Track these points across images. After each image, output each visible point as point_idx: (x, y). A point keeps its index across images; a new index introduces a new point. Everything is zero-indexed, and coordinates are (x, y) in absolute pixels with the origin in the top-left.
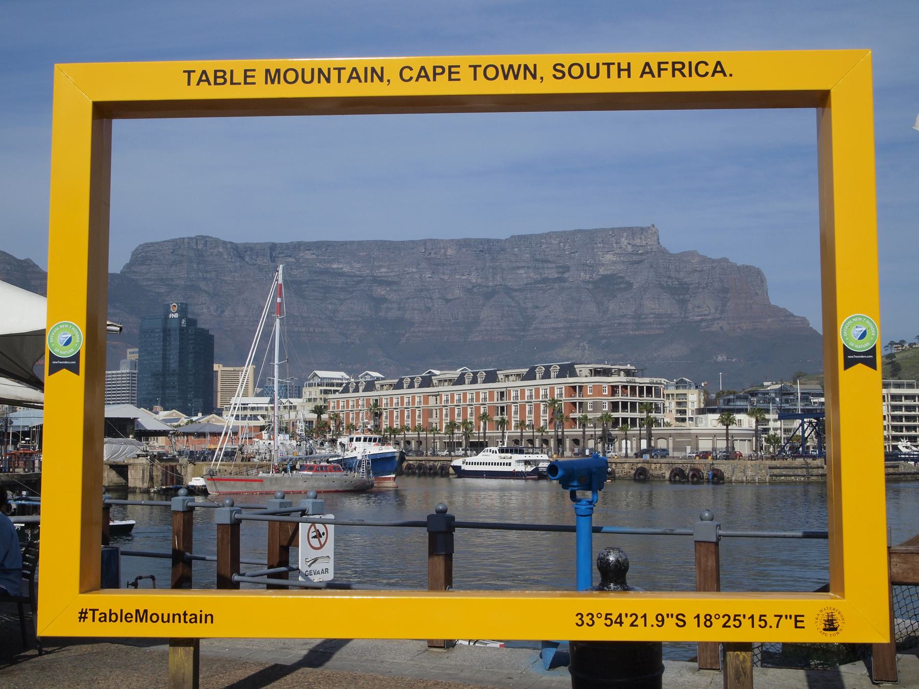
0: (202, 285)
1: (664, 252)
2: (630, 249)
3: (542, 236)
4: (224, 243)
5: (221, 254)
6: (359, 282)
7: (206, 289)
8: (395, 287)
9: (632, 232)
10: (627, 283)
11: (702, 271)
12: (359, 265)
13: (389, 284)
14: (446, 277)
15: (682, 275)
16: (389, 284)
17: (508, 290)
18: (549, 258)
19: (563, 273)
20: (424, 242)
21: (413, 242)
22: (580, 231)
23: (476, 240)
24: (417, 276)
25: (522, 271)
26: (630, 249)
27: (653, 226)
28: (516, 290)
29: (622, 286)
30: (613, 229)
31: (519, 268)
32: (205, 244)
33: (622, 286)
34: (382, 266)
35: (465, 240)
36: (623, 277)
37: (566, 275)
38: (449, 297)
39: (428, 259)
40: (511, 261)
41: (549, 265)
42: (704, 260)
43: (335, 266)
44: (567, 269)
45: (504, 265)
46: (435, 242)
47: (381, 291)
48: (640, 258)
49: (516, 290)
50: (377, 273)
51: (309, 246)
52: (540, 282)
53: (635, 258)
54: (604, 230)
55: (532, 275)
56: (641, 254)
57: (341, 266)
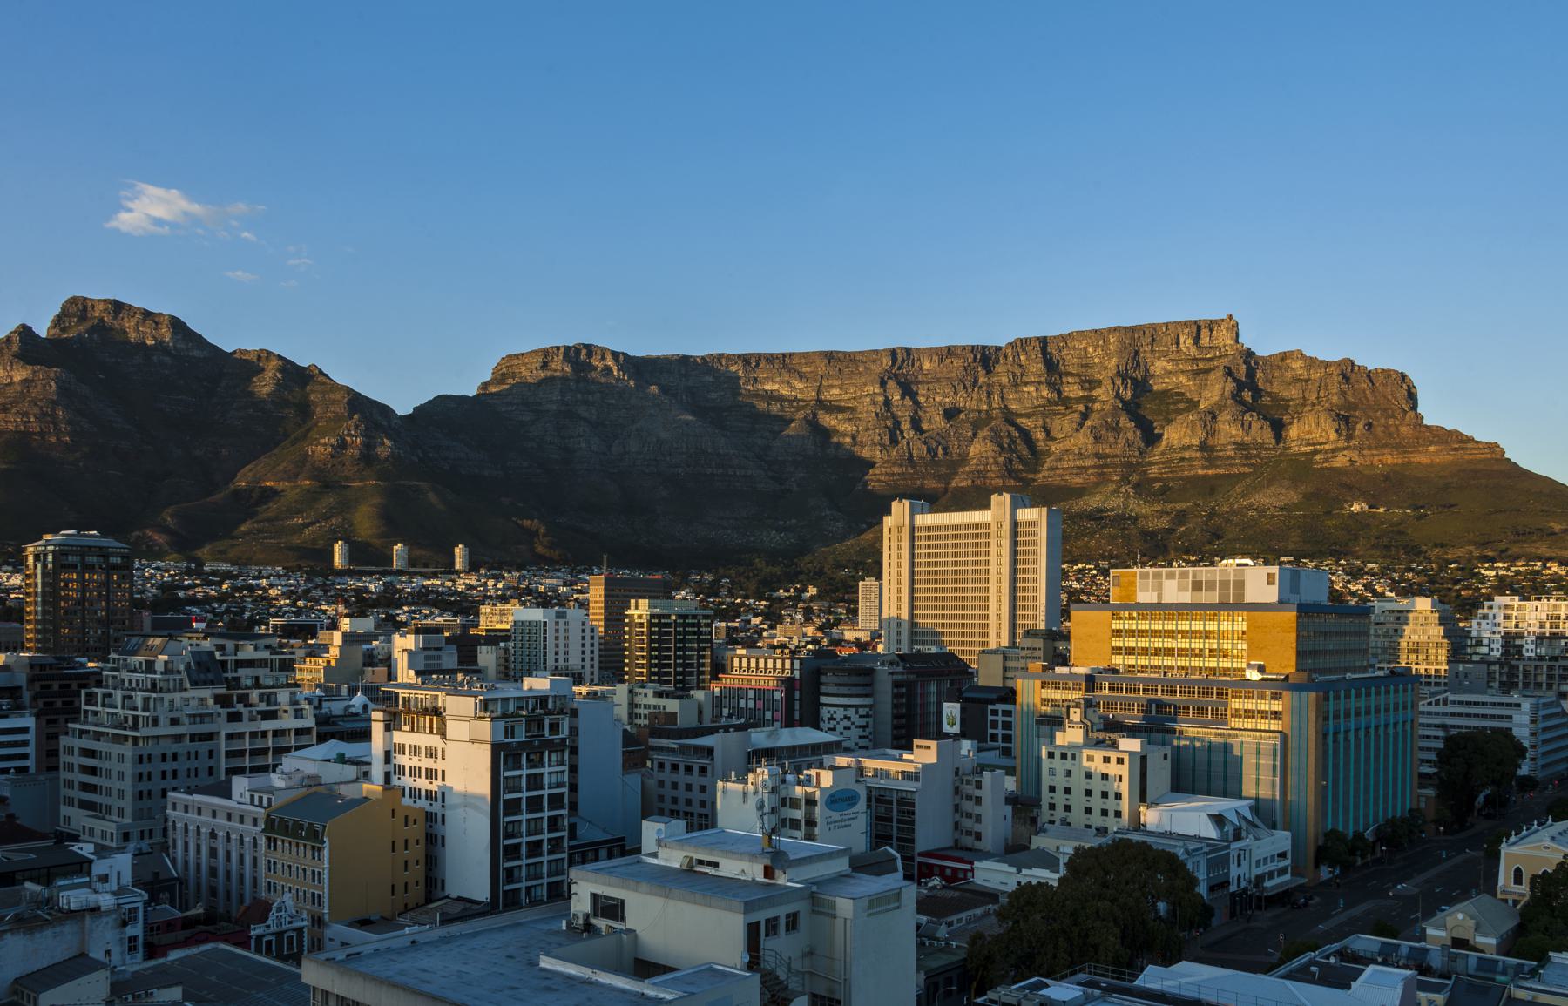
0: (582, 411)
1: (1249, 354)
2: (1194, 351)
3: (1063, 338)
4: (615, 355)
5: (608, 370)
6: (803, 408)
7: (585, 414)
8: (847, 415)
9: (1197, 328)
10: (1190, 401)
11: (1307, 381)
12: (800, 386)
13: (841, 410)
14: (922, 400)
15: (1275, 389)
16: (841, 410)
17: (1009, 417)
18: (1070, 369)
19: (1091, 389)
20: (893, 353)
21: (876, 352)
22: (1115, 329)
23: (964, 348)
24: (881, 399)
25: (1032, 389)
26: (1194, 351)
27: (1231, 317)
28: (1021, 416)
29: (1182, 406)
30: (1167, 325)
31: (1026, 384)
32: (590, 355)
33: (1182, 406)
34: (832, 387)
35: (949, 348)
36: (1182, 394)
37: (1094, 393)
38: (925, 426)
39: (896, 376)
40: (1014, 375)
41: (1070, 380)
42: (1311, 363)
43: (768, 387)
44: (1099, 383)
45: (1005, 380)
46: (908, 351)
47: (828, 420)
48: (1211, 365)
49: (1021, 416)
50: (826, 396)
51: (731, 358)
52: (1056, 404)
53: (1201, 366)
54: (1154, 327)
55: (1045, 392)
56: (1211, 359)
57: (776, 387)
